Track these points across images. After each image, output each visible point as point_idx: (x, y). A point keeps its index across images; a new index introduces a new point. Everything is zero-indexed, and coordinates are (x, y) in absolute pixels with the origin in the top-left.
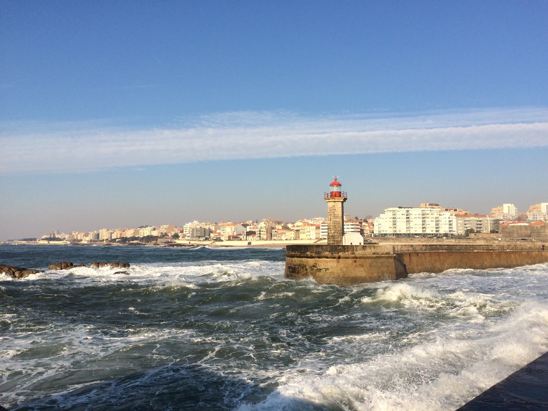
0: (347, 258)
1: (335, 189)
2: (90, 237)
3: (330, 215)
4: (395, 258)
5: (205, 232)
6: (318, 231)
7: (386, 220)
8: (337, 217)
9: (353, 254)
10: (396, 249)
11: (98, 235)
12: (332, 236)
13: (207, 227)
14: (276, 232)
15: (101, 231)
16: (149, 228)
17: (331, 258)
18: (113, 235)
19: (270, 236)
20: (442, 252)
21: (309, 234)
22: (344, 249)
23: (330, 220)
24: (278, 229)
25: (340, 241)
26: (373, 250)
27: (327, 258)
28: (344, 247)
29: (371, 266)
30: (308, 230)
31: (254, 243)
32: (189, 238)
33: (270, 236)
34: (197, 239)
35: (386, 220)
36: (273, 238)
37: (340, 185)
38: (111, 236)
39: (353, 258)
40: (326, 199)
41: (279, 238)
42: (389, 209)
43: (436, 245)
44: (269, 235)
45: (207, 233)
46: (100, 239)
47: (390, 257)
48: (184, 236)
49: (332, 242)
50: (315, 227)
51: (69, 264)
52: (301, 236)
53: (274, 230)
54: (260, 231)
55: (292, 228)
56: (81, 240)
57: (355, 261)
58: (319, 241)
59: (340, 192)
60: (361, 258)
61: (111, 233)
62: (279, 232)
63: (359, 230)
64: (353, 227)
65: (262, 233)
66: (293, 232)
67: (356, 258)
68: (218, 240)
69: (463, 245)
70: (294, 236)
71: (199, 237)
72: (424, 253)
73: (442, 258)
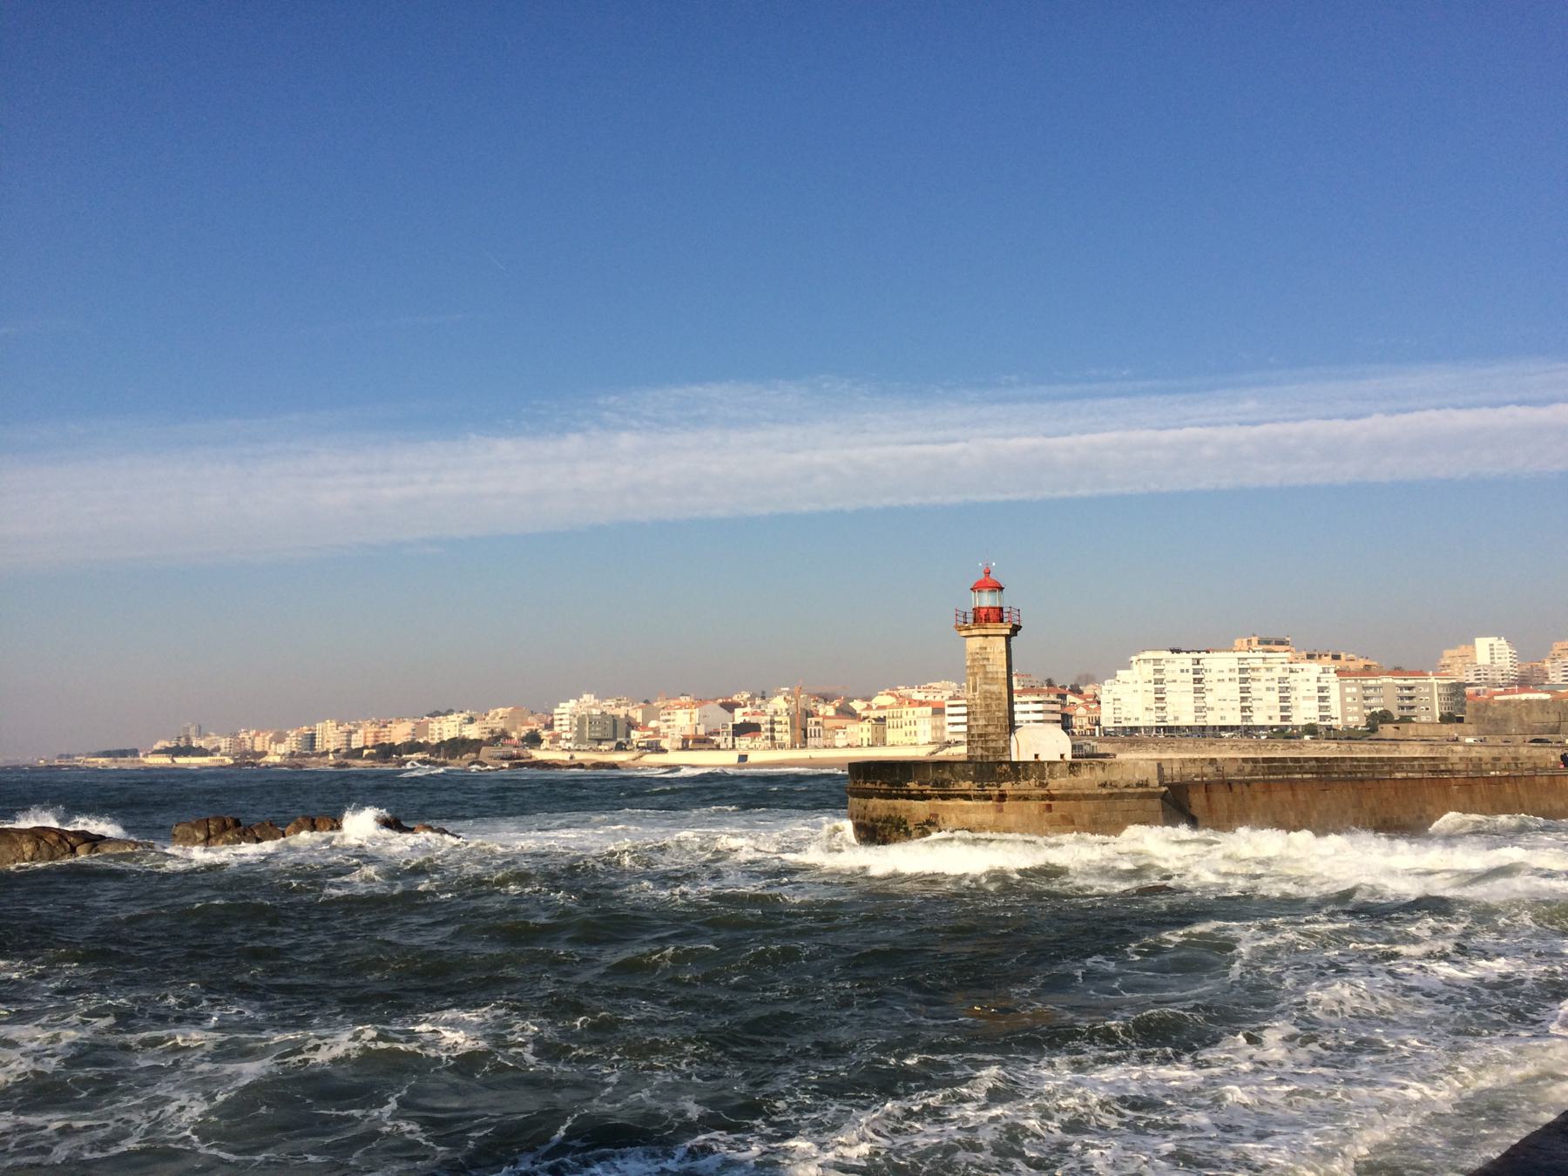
0: (1026, 798)
1: (987, 600)
2: (291, 744)
3: (974, 674)
4: (1164, 796)
5: (615, 726)
6: (938, 721)
7: (1136, 687)
8: (994, 680)
10: (1167, 772)
11: (313, 738)
12: (980, 736)
13: (621, 712)
14: (817, 723)
15: (319, 726)
16: (455, 718)
17: (977, 797)
18: (354, 737)
19: (802, 738)
20: (1303, 780)
21: (913, 728)
22: (1017, 772)
23: (975, 690)
24: (825, 717)
25: (1004, 749)
26: (1100, 775)
27: (967, 797)
28: (1014, 765)
30: (911, 717)
31: (754, 757)
32: (570, 745)
33: (802, 738)
34: (595, 746)
35: (1136, 687)
36: (811, 741)
37: (1001, 589)
38: (349, 741)
39: (1043, 798)
40: (959, 629)
41: (828, 742)
42: (1142, 656)
43: (1283, 760)
44: (799, 732)
45: (621, 728)
46: (319, 747)
47: (1151, 796)
48: (556, 739)
49: (979, 752)
50: (929, 710)
51: (229, 823)
52: (891, 736)
53: (813, 720)
54: (772, 722)
55: (864, 714)
56: (265, 754)
57: (1049, 808)
58: (941, 749)
59: (1001, 609)
60: (1064, 797)
61: (350, 733)
62: (829, 723)
63: (1059, 717)
64: (1040, 707)
65: (777, 727)
66: (866, 725)
67: (1052, 797)
68: (656, 748)
69: (1363, 759)
70: (869, 735)
71: (600, 741)
72: (1248, 784)
73: (1301, 797)
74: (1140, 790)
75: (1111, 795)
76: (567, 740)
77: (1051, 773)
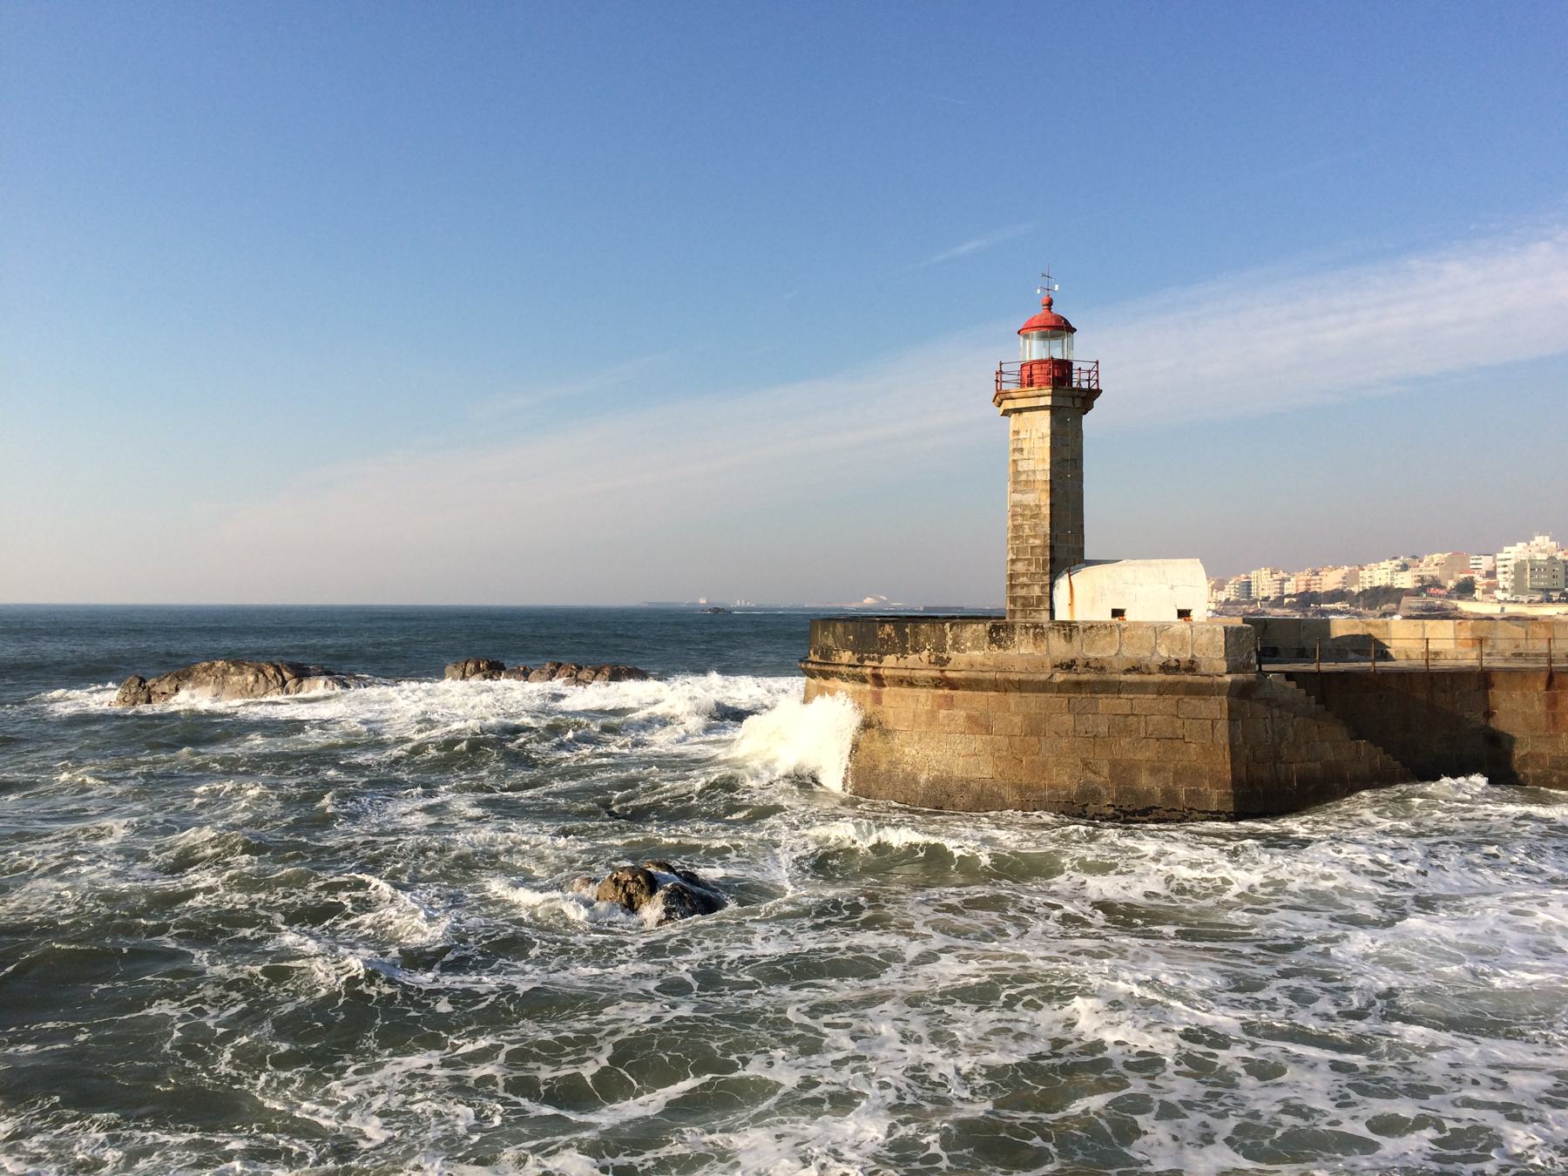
0: (911, 683)
9: (942, 662)
11: (1249, 585)
15: (1253, 574)
18: (1286, 585)
22: (903, 637)
25: (1040, 599)
26: (1058, 647)
29: (1035, 729)
32: (1507, 596)
38: (1282, 589)
48: (1489, 590)
61: (1283, 581)
67: (952, 685)
74: (1158, 677)
75: (1078, 686)
76: (1504, 589)
77: (955, 642)
